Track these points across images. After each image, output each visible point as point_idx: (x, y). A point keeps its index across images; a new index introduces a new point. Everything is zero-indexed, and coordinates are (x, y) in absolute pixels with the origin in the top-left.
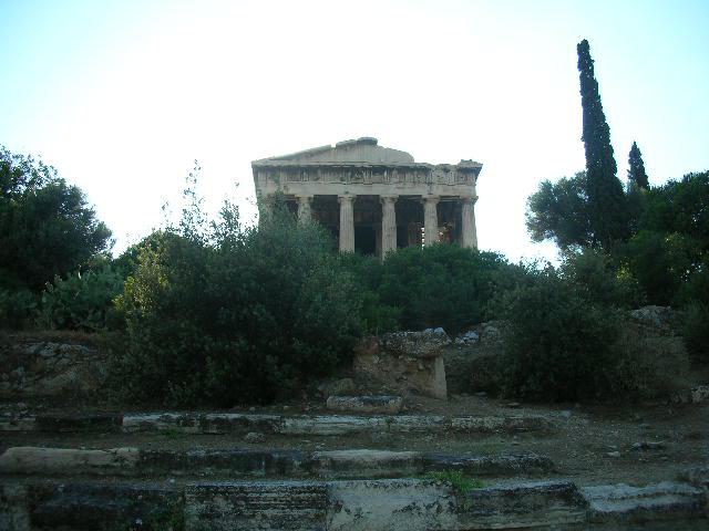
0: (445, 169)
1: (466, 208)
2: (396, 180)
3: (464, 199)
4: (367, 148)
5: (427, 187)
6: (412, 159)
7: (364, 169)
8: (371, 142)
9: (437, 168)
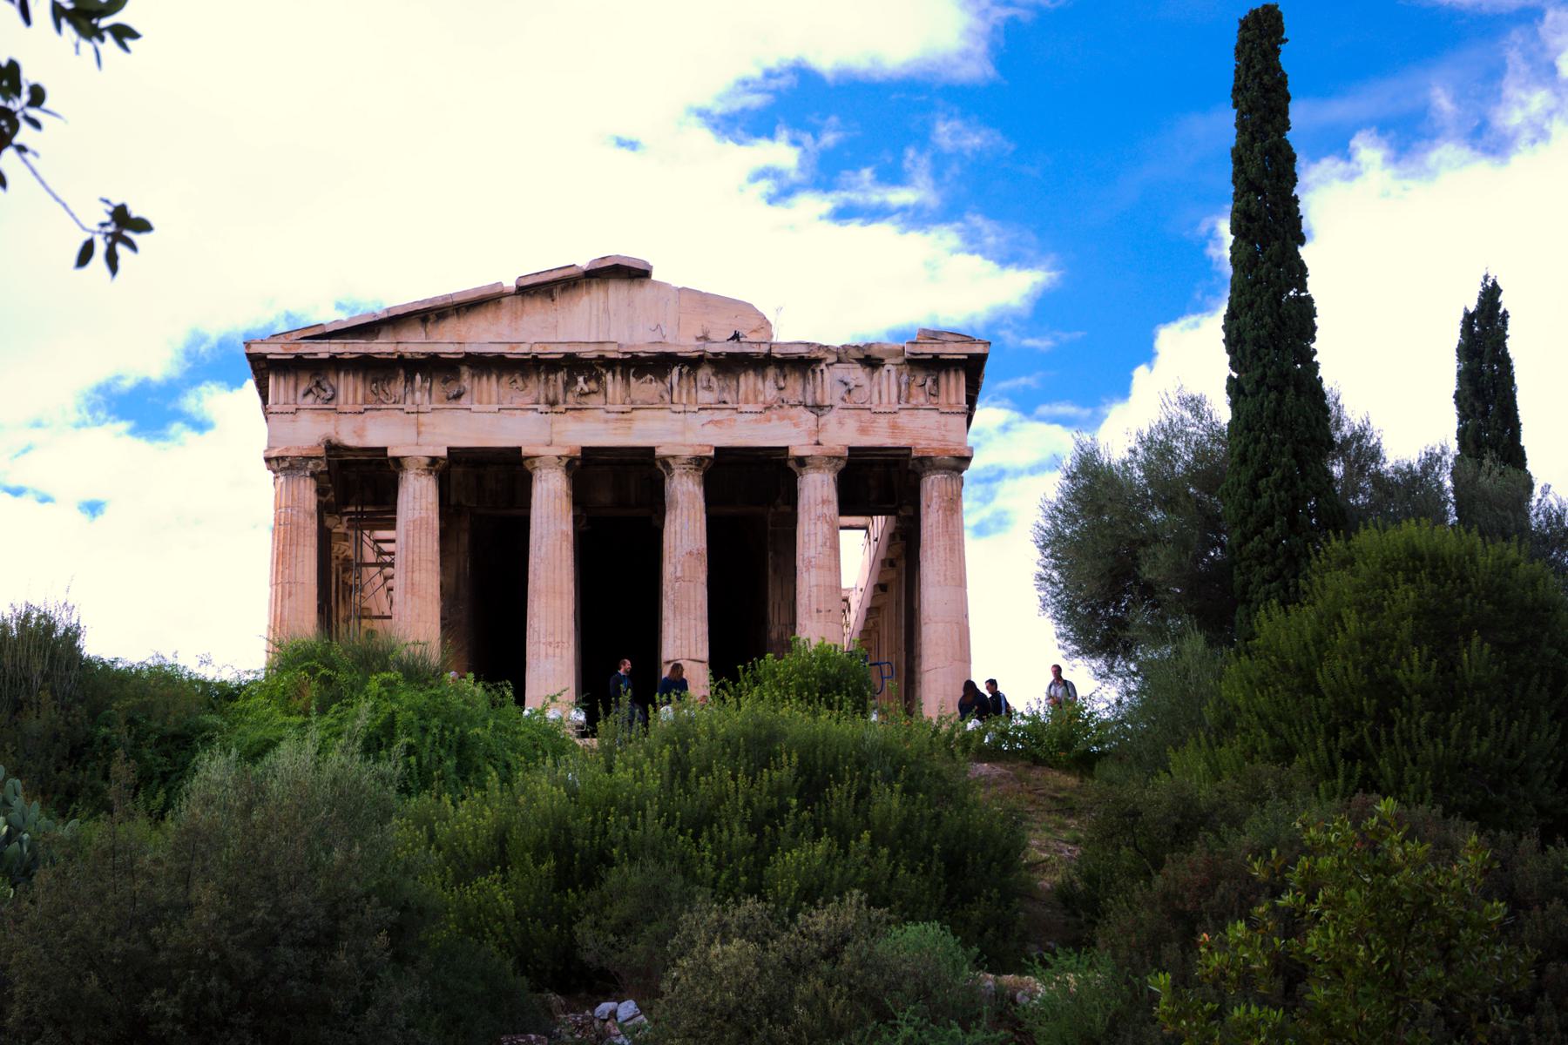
0: (870, 360)
1: (933, 487)
2: (705, 397)
3: (921, 460)
4: (617, 293)
5: (808, 417)
6: (765, 324)
7: (609, 364)
8: (631, 273)
9: (842, 355)
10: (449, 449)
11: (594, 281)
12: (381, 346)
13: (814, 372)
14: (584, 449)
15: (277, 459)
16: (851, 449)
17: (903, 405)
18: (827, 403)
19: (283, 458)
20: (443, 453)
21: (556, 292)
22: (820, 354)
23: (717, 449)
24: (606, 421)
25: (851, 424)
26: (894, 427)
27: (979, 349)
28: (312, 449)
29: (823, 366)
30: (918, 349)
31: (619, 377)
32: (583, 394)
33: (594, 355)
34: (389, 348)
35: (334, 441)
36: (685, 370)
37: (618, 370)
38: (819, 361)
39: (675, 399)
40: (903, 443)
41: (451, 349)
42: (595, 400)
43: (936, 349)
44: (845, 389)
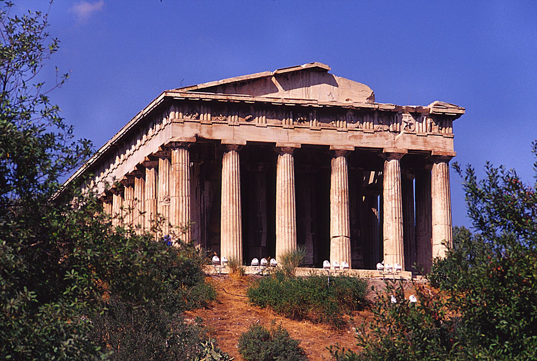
7: (310, 109)
10: (247, 141)
11: (304, 72)
12: (220, 97)
13: (394, 117)
15: (176, 142)
16: (408, 150)
17: (429, 133)
18: (398, 130)
19: (179, 142)
20: (245, 143)
23: (355, 147)
24: (310, 133)
25: (408, 139)
26: (425, 142)
27: (461, 112)
28: (191, 138)
30: (437, 110)
32: (300, 121)
34: (225, 98)
38: (396, 113)
39: (338, 126)
40: (429, 149)
41: (251, 99)
43: (444, 111)
44: (406, 124)
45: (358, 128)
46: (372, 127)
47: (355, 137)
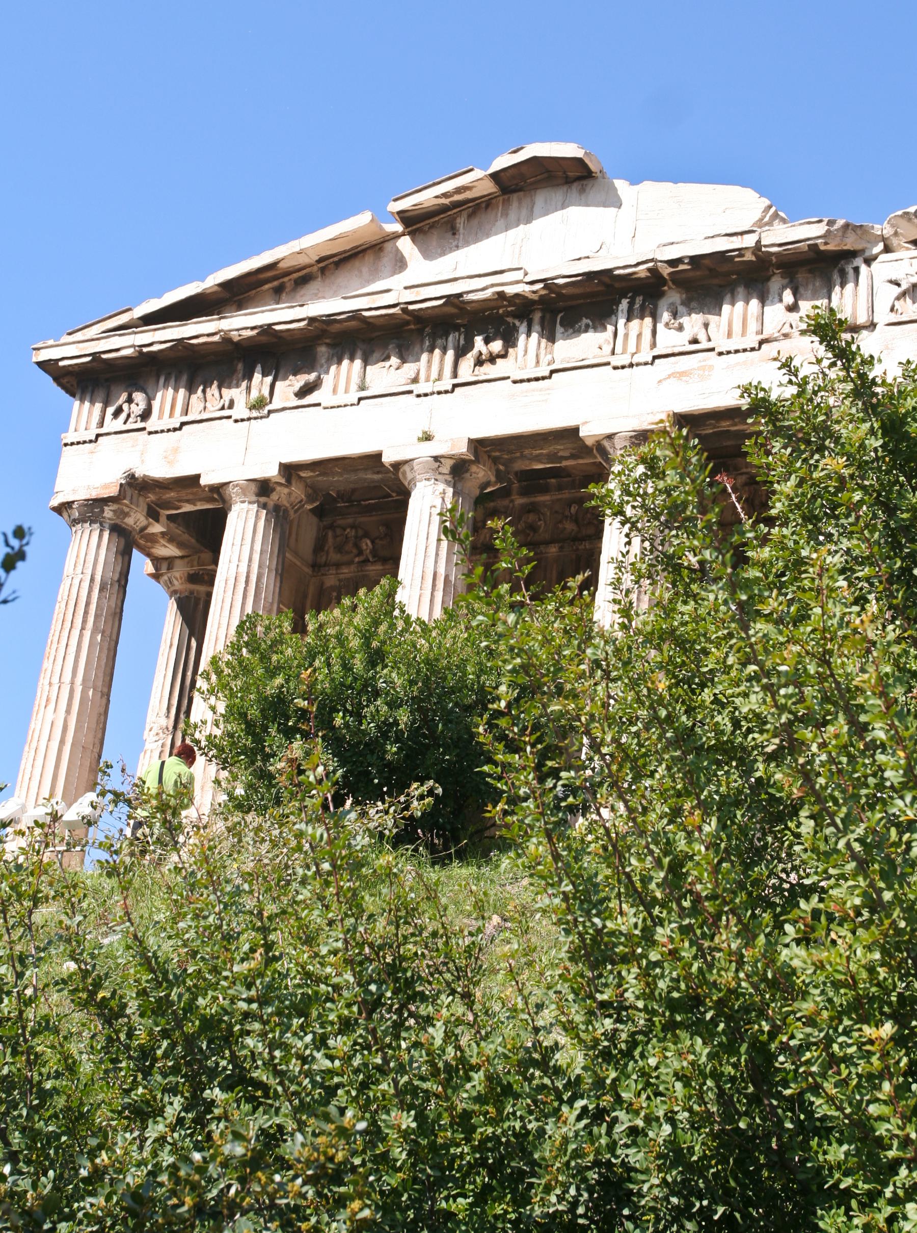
2: (669, 339)
11: (515, 196)
12: (200, 329)
14: (471, 442)
18: (862, 319)
21: (460, 222)
22: (850, 243)
28: (106, 486)
29: (859, 262)
31: (536, 327)
32: (479, 362)
33: (488, 294)
35: (140, 471)
36: (639, 300)
37: (537, 316)
38: (852, 254)
39: (618, 349)
42: (501, 368)
45: (695, 341)
46: (753, 326)
47: (680, 375)
